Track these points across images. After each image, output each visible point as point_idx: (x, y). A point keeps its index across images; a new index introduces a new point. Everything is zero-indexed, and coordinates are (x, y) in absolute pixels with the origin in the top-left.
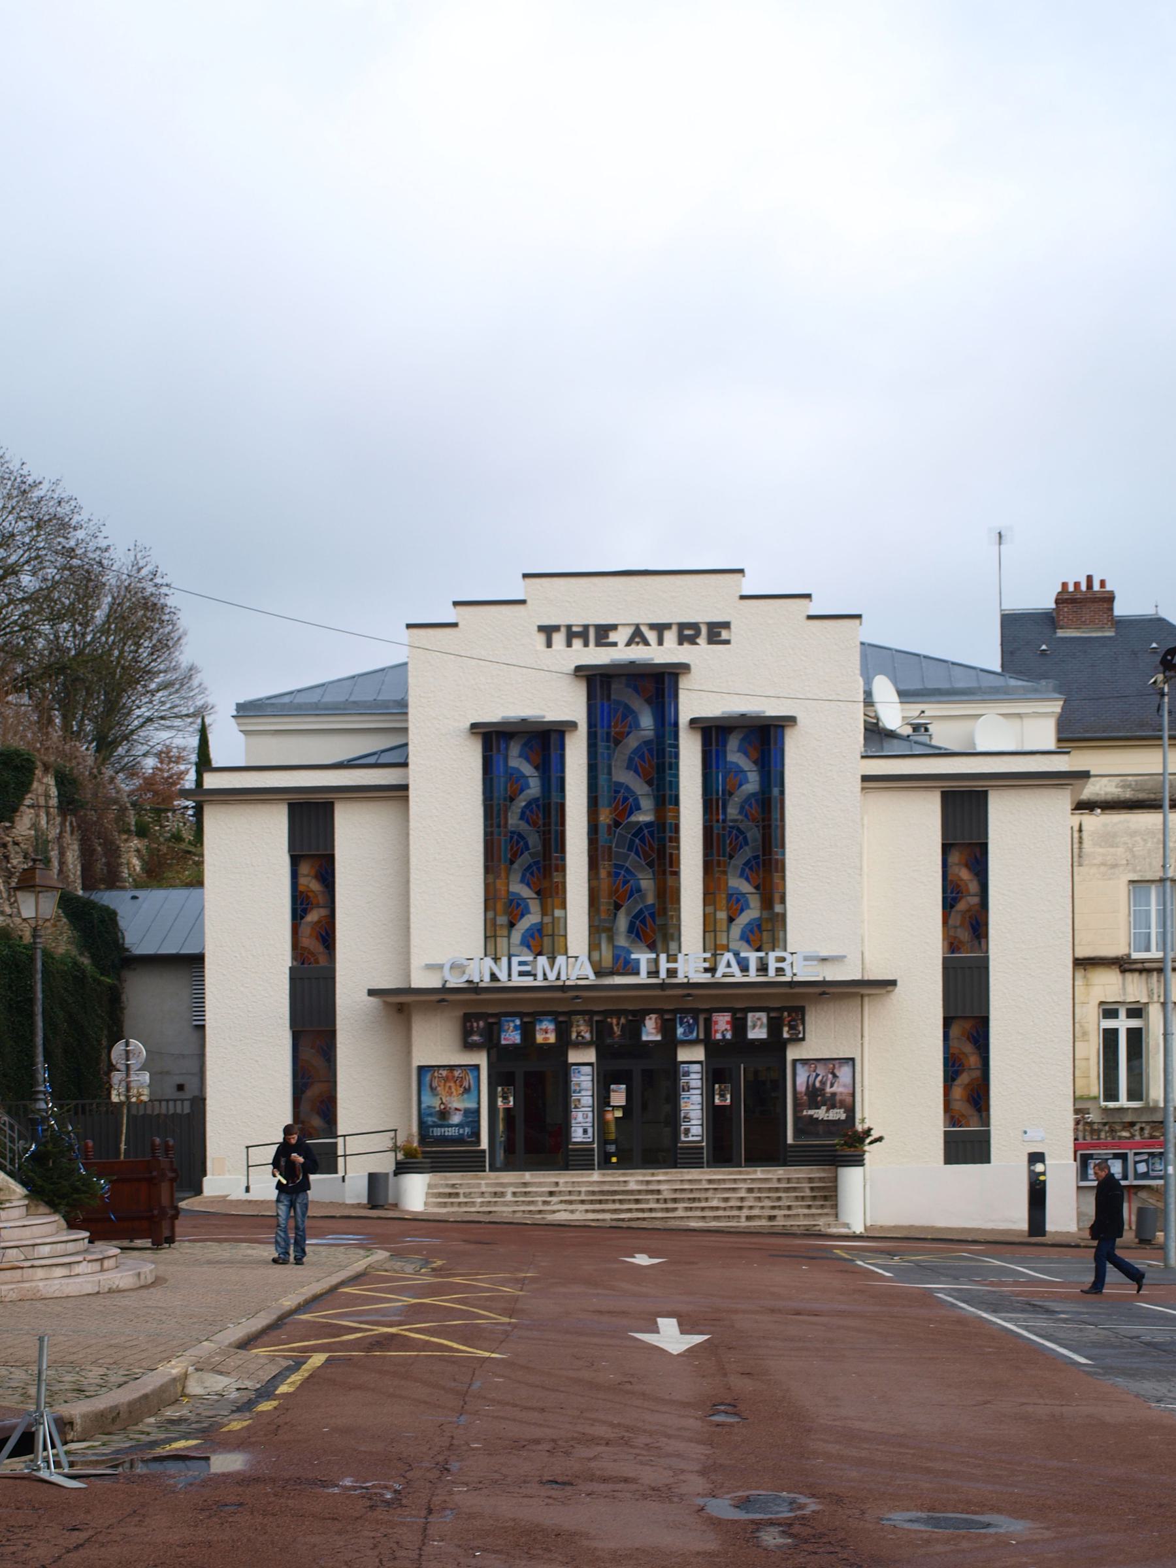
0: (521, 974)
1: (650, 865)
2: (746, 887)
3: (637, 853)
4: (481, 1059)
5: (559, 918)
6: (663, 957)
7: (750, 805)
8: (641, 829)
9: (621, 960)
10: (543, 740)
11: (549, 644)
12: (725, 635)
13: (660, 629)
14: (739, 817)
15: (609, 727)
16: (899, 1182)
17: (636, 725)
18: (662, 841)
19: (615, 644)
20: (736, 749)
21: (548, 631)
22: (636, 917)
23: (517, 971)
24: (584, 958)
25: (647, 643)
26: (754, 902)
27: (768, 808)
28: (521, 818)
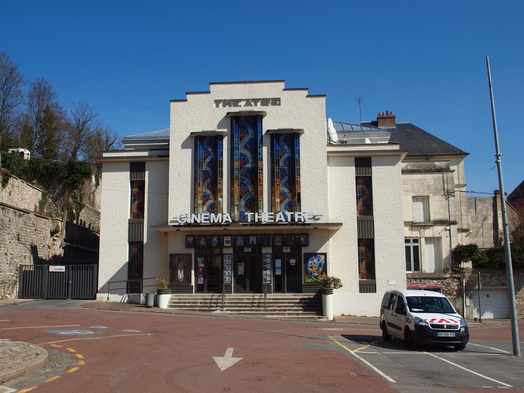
0: (205, 220)
2: (286, 190)
3: (248, 178)
4: (192, 251)
6: (256, 214)
9: (242, 216)
11: (217, 106)
13: (256, 101)
16: (347, 302)
19: (241, 106)
21: (217, 102)
22: (247, 201)
23: (202, 217)
25: (251, 106)
28: (208, 166)
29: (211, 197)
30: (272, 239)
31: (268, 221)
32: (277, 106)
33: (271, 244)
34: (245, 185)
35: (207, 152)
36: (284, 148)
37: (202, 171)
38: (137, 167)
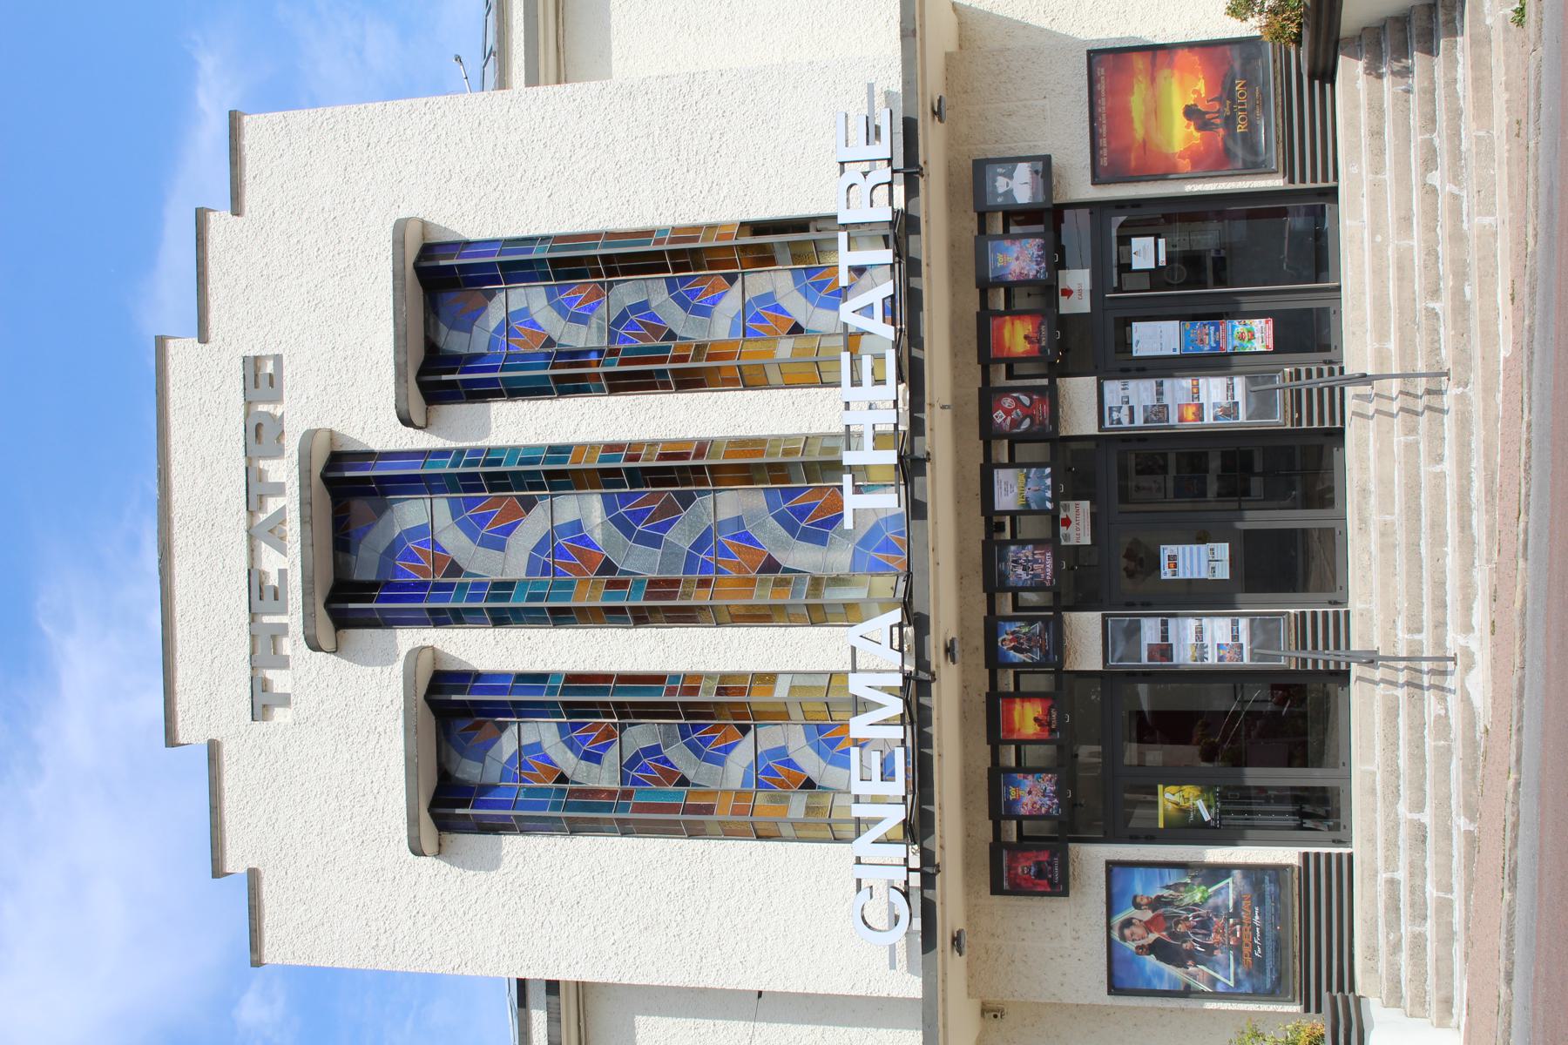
1: (687, 500)
2: (731, 303)
3: (666, 527)
4: (1093, 857)
5: (792, 688)
7: (571, 301)
8: (618, 522)
10: (454, 712)
11: (285, 700)
12: (269, 368)
13: (256, 491)
14: (594, 322)
15: (423, 586)
17: (424, 532)
18: (640, 477)
19: (283, 574)
20: (466, 336)
21: (262, 703)
22: (791, 529)
24: (849, 635)
26: (759, 282)
27: (573, 265)
29: (770, 736)
31: (893, 391)
32: (286, 373)
33: (1045, 382)
34: (699, 545)
35: (523, 765)
36: (498, 330)
37: (627, 795)
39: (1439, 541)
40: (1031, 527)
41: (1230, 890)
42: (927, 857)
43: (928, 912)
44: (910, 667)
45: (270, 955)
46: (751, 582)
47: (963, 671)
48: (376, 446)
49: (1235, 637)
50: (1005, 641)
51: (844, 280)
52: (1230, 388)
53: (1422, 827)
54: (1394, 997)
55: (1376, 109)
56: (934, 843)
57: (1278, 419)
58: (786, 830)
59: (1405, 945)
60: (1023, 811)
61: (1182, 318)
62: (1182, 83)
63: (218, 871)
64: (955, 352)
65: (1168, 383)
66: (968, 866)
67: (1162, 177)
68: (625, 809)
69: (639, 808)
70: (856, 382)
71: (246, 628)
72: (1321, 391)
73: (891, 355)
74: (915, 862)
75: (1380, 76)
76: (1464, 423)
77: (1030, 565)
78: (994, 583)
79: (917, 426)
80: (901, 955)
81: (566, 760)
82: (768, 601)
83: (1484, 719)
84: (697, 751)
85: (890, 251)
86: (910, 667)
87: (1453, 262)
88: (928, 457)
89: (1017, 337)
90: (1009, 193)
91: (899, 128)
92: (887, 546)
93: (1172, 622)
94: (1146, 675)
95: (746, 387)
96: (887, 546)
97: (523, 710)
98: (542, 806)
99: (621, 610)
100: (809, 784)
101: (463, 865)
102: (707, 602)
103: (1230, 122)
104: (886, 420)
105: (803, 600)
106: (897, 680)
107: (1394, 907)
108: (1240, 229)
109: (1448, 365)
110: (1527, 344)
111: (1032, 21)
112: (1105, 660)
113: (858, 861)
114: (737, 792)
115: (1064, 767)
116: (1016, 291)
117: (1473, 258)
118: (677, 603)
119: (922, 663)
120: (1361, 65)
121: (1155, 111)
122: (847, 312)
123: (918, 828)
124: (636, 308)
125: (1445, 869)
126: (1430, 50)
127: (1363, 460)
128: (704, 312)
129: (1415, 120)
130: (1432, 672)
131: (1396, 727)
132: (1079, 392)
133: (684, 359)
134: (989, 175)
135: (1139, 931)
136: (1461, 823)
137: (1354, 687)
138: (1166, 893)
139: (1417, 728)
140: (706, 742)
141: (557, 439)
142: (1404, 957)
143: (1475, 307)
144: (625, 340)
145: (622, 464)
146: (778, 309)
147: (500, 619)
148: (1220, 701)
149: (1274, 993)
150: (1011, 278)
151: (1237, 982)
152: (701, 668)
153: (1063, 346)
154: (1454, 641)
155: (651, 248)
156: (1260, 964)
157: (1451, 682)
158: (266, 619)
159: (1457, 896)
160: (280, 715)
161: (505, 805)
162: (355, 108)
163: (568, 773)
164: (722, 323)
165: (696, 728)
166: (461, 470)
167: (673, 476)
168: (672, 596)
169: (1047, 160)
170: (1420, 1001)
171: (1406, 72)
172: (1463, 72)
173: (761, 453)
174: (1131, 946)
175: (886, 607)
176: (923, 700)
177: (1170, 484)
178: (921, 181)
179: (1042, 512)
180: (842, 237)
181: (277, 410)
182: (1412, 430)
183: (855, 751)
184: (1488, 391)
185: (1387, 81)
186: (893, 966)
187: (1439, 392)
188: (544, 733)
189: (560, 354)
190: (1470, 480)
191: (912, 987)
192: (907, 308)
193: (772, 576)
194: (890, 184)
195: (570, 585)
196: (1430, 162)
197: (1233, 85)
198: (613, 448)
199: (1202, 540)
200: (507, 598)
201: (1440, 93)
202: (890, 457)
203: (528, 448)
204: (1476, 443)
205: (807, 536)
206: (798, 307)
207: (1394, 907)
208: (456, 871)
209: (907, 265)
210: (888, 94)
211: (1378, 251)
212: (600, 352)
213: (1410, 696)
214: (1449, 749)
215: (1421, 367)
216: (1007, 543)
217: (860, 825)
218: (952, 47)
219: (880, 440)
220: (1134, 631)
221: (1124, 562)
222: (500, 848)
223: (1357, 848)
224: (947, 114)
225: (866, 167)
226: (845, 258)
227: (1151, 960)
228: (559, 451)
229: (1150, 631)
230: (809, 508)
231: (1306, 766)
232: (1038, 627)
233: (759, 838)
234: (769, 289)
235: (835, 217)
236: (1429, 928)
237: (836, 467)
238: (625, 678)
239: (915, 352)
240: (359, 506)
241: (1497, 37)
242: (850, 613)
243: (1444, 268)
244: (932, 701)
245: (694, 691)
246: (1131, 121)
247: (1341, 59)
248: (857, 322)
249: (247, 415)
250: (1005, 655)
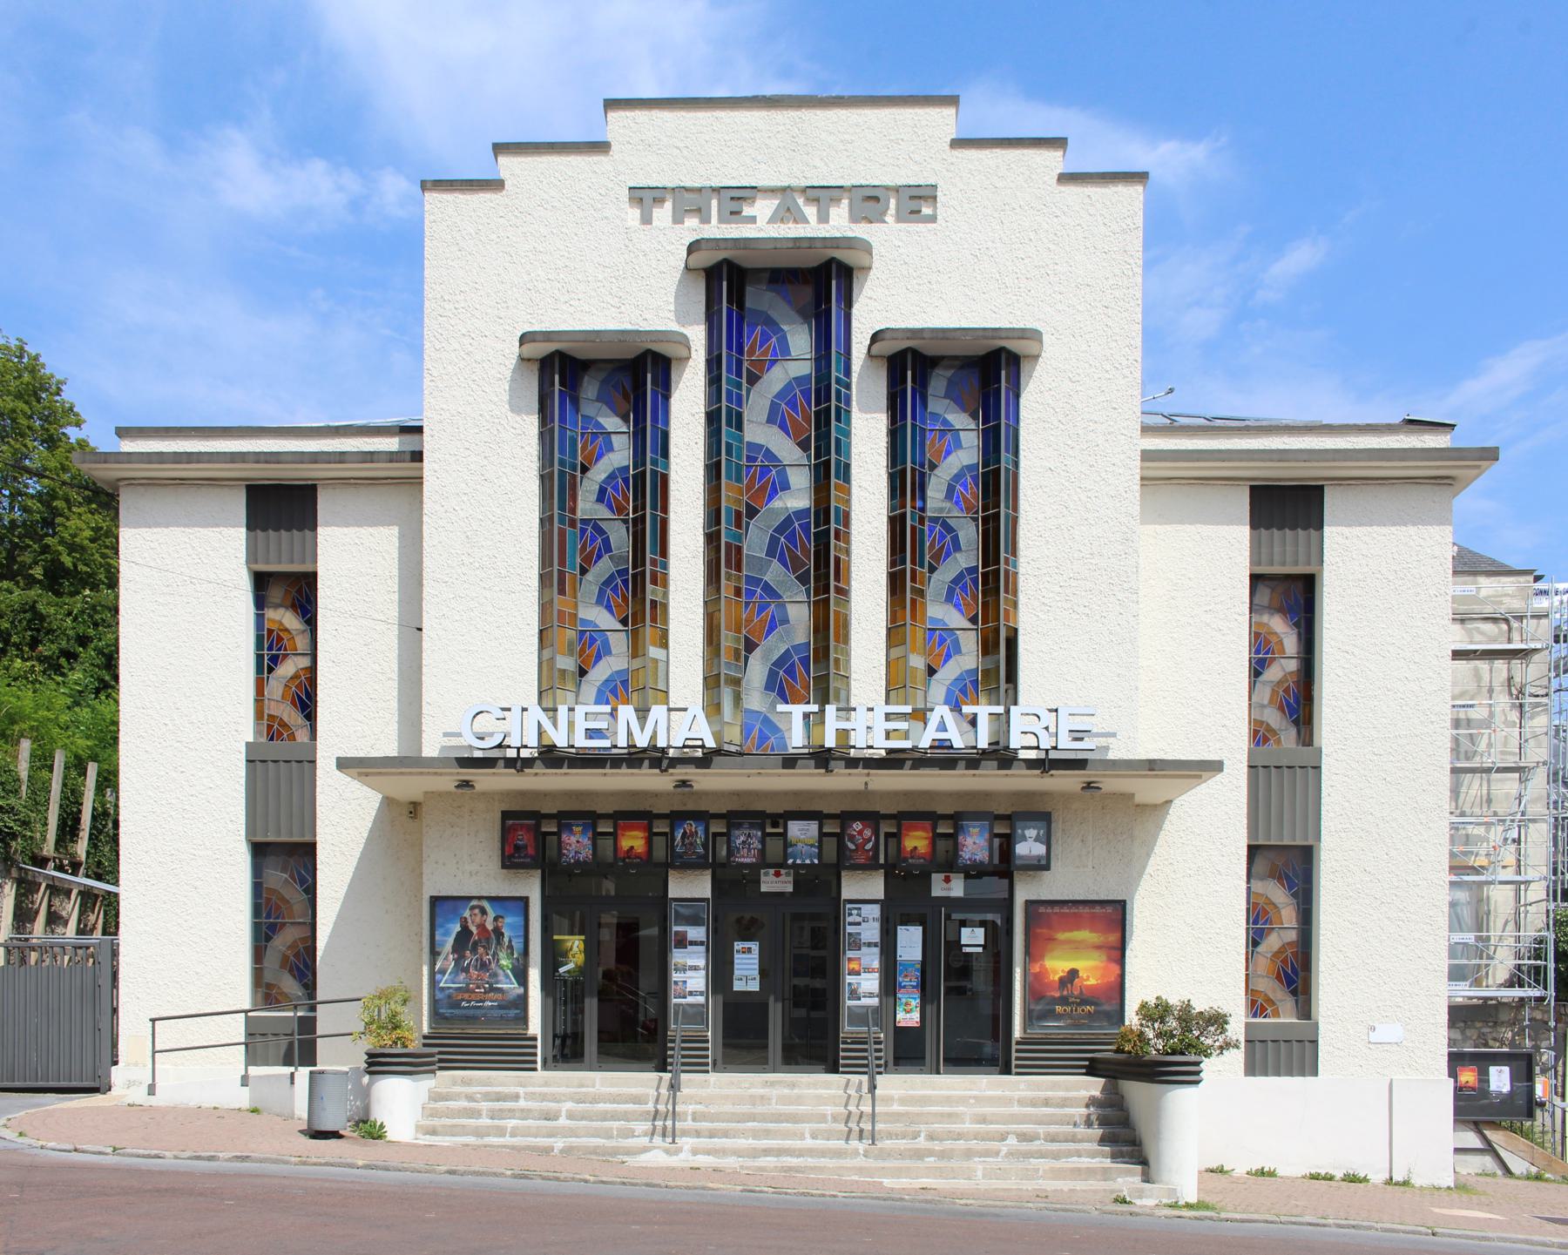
1: (803, 579)
3: (783, 562)
4: (531, 888)
5: (656, 661)
7: (965, 486)
8: (788, 521)
10: (638, 374)
11: (646, 220)
13: (822, 195)
14: (948, 505)
15: (740, 351)
19: (753, 220)
21: (645, 197)
22: (779, 663)
25: (801, 219)
26: (970, 642)
27: (994, 487)
30: (888, 835)
32: (921, 227)
33: (882, 861)
34: (767, 588)
36: (945, 422)
37: (573, 523)
38: (281, 506)
39: (756, 1135)
40: (774, 846)
41: (510, 986)
42: (529, 763)
43: (487, 763)
44: (671, 753)
45: (433, 199)
46: (738, 631)
47: (668, 794)
48: (856, 310)
49: (691, 993)
50: (691, 826)
51: (967, 709)
52: (871, 995)
53: (556, 1118)
54: (436, 1097)
55: (1064, 1103)
56: (539, 769)
57: (847, 1028)
58: (547, 653)
59: (473, 1105)
60: (564, 837)
61: (924, 962)
62: (1096, 968)
63: (499, 149)
64: (907, 794)
65: (876, 950)
66: (522, 794)
67: (1028, 951)
68: (562, 521)
69: (562, 533)
70: (888, 717)
71: (708, 184)
72: (865, 1058)
73: (907, 744)
74: (525, 753)
75: (1087, 1106)
76: (838, 1154)
77: (746, 846)
78: (734, 819)
79: (853, 763)
80: (454, 742)
81: (599, 473)
82: (724, 643)
83: (632, 1161)
84: (607, 583)
85: (986, 746)
86: (671, 753)
87: (952, 1150)
88: (829, 771)
89: (916, 841)
90: (1024, 838)
91: (1080, 756)
92: (763, 738)
93: (703, 948)
94: (664, 930)
95: (889, 630)
96: (763, 738)
97: (639, 437)
98: (562, 451)
99: (718, 522)
100: (583, 672)
101: (513, 380)
102: (723, 594)
103: (1064, 1001)
104: (858, 739)
105: (724, 671)
106: (661, 743)
107: (499, 1098)
108: (986, 1008)
109: (879, 1145)
110: (891, 1197)
111: (1152, 861)
112: (676, 900)
113: (524, 710)
114: (576, 615)
115: (595, 868)
116: (951, 842)
117: (954, 1164)
118: (723, 569)
119: (674, 762)
120: (1097, 1093)
121: (1077, 947)
122: (942, 711)
123: (550, 756)
124: (956, 540)
125: (527, 1133)
126: (1103, 1141)
127: (815, 1086)
128: (949, 597)
129: (1054, 1128)
130: (665, 1128)
131: (626, 1102)
132: (874, 887)
133: (913, 579)
134: (1040, 824)
135: (478, 919)
136: (559, 1144)
137: (655, 1075)
138: (506, 939)
139: (626, 1116)
140: (615, 590)
141: (854, 471)
142: (464, 1104)
143: (919, 1164)
144: (931, 530)
145: (833, 526)
146: (948, 657)
147: (712, 418)
148: (646, 983)
149: (436, 1015)
150: (961, 838)
151: (443, 989)
152: (672, 588)
153: (908, 876)
154: (686, 1143)
155: (1003, 555)
156: (457, 1005)
157: (657, 1140)
158: (714, 203)
159: (507, 1140)
160: (636, 213)
161: (562, 420)
162: (1139, 295)
163: (589, 474)
164: (940, 612)
165: (625, 582)
166: (834, 386)
167: (822, 569)
168: (728, 565)
169: (1047, 867)
170: (434, 1114)
171: (1089, 1124)
172: (1085, 1162)
173: (837, 640)
174: (467, 914)
175: (717, 736)
176: (646, 763)
177: (805, 951)
178: (1038, 772)
179: (786, 857)
180: (1000, 709)
181: (890, 218)
182: (835, 1119)
183: (608, 709)
184: (860, 1171)
185: (1084, 1111)
186: (446, 735)
187: (861, 1138)
188: (620, 455)
189: (923, 475)
190: (798, 1156)
191: (430, 749)
192: (943, 758)
193: (742, 647)
194: (1038, 748)
195: (739, 480)
196: (1024, 1137)
197: (1091, 1004)
198: (846, 519)
199: (762, 972)
200: (729, 424)
201: (1072, 1146)
202: (830, 742)
203: (849, 445)
204: (824, 1162)
205: (772, 675)
206: (949, 673)
207: (499, 1098)
208: (508, 374)
209: (974, 760)
210: (1107, 748)
211: (963, 1100)
212: (923, 509)
213: (648, 1112)
214: (611, 1137)
215: (879, 1126)
216: (763, 829)
217: (552, 711)
218: (1138, 799)
219: (843, 734)
220: (694, 921)
221: (747, 916)
222: (528, 413)
223: (541, 1074)
224: (1088, 793)
225: (1052, 729)
226: (983, 711)
227: (458, 928)
228: (845, 472)
229: (696, 933)
230: (794, 679)
231: (600, 1040)
232: (701, 850)
233: (541, 632)
234: (964, 650)
235: (1016, 703)
236: (485, 1121)
237: (824, 700)
238: (664, 524)
239: (909, 763)
240: (807, 293)
241: (1109, 1185)
242: (713, 708)
243: (948, 1144)
244: (645, 770)
245: (654, 582)
246: (1071, 930)
247: (1102, 1080)
248: (933, 720)
249: (887, 188)
250: (680, 826)
